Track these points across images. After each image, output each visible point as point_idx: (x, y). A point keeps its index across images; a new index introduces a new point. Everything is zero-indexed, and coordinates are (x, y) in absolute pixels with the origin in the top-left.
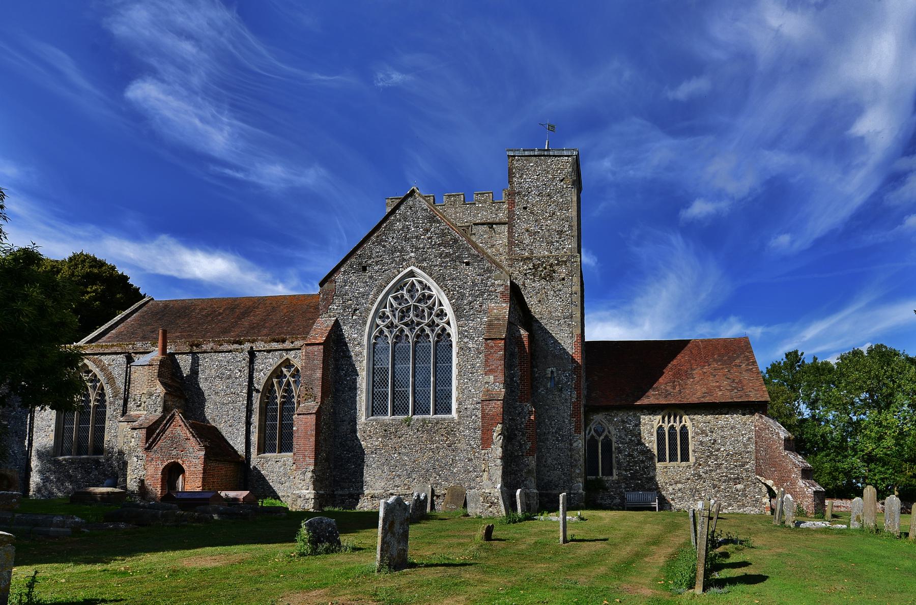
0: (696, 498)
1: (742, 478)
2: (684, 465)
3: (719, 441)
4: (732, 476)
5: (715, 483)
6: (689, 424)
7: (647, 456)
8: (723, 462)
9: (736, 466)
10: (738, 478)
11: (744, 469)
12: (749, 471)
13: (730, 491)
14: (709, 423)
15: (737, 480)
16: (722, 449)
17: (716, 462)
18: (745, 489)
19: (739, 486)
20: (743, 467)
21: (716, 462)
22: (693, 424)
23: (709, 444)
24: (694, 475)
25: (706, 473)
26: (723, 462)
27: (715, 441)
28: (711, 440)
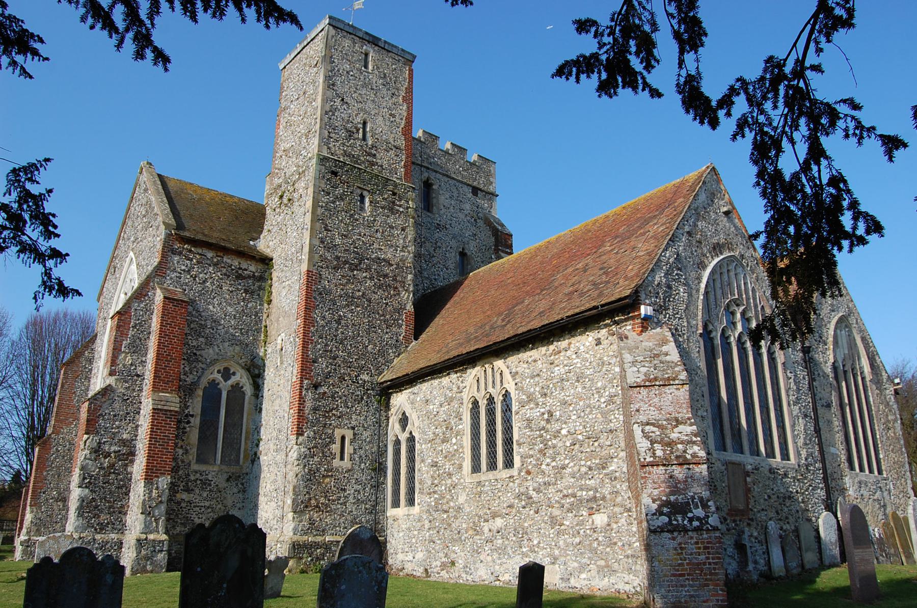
0: (524, 550)
1: (604, 498)
2: (504, 476)
3: (558, 413)
4: (584, 493)
5: (556, 512)
6: (510, 386)
7: (455, 463)
8: (567, 462)
9: (590, 469)
10: (594, 499)
11: (607, 474)
12: (615, 478)
13: (582, 532)
14: (538, 375)
15: (594, 504)
16: (564, 432)
17: (554, 464)
18: (609, 525)
19: (600, 519)
20: (604, 468)
21: (554, 464)
22: (516, 384)
23: (543, 423)
24: (518, 497)
25: (538, 491)
26: (567, 462)
27: (551, 414)
28: (543, 414)
